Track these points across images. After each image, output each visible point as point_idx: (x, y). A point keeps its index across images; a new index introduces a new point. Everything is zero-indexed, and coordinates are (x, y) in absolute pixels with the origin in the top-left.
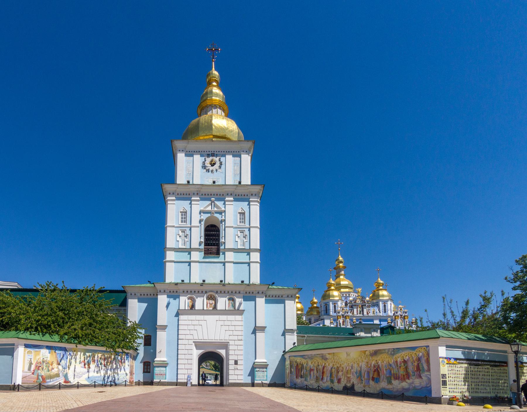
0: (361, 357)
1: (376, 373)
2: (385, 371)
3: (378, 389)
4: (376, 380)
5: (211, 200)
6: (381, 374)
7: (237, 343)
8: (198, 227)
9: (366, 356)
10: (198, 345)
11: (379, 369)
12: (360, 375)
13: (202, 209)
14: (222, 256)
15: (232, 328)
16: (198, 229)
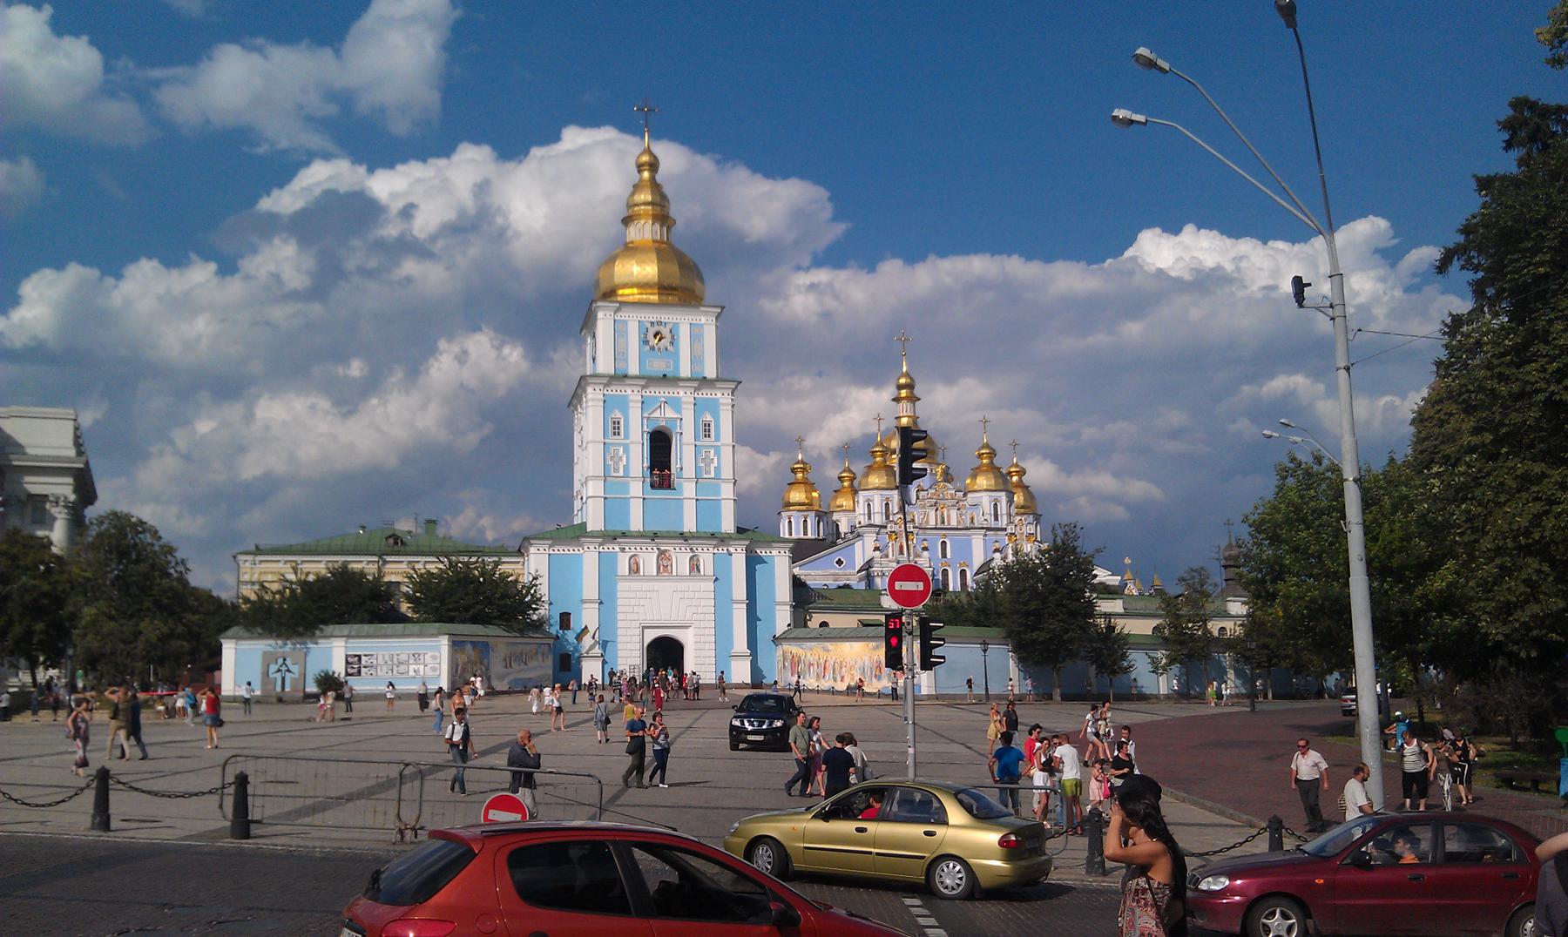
13: (646, 415)
15: (695, 602)
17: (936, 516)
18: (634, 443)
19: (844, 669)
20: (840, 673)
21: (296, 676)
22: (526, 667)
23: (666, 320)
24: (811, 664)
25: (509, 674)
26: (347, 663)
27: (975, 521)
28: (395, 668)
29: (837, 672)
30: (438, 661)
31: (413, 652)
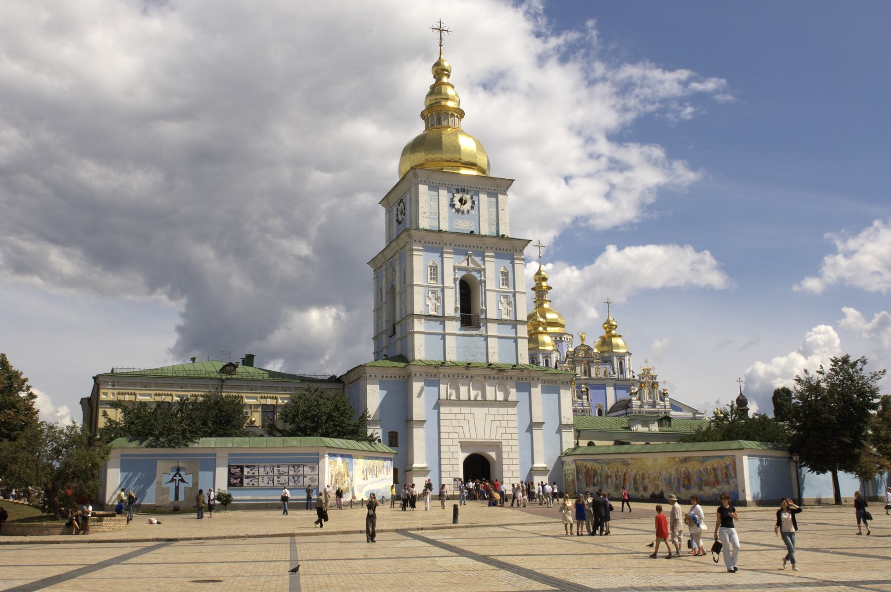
0: (670, 464)
1: (686, 480)
2: (695, 478)
3: (689, 495)
4: (688, 487)
5: (467, 254)
6: (691, 481)
7: (511, 443)
8: (451, 288)
9: (676, 462)
10: (464, 445)
11: (690, 476)
12: (669, 482)
13: (457, 264)
14: (483, 329)
15: (504, 424)
16: (453, 291)
17: (581, 369)
18: (448, 287)
19: (646, 480)
20: (642, 483)
21: (190, 485)
22: (376, 479)
23: (469, 188)
24: (608, 477)
25: (366, 485)
26: (230, 473)
27: (607, 374)
28: (276, 478)
29: (639, 483)
30: (316, 473)
31: (294, 464)
